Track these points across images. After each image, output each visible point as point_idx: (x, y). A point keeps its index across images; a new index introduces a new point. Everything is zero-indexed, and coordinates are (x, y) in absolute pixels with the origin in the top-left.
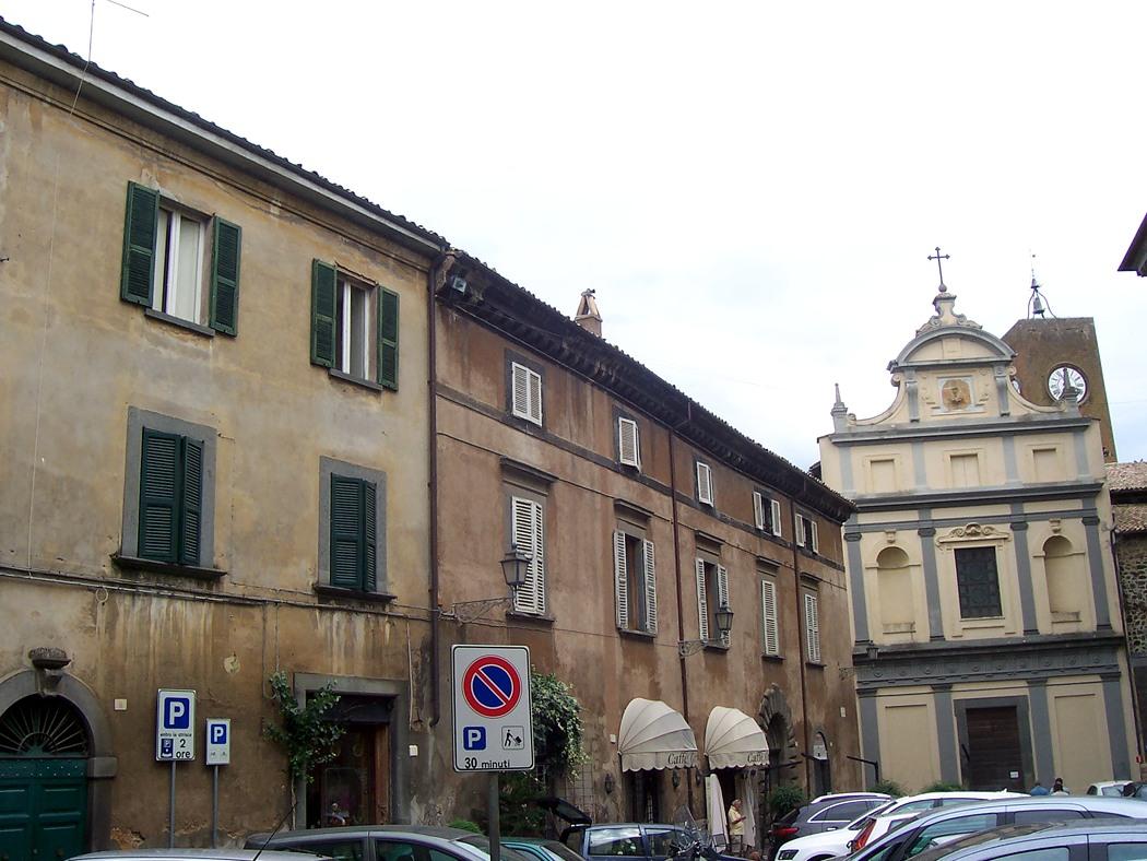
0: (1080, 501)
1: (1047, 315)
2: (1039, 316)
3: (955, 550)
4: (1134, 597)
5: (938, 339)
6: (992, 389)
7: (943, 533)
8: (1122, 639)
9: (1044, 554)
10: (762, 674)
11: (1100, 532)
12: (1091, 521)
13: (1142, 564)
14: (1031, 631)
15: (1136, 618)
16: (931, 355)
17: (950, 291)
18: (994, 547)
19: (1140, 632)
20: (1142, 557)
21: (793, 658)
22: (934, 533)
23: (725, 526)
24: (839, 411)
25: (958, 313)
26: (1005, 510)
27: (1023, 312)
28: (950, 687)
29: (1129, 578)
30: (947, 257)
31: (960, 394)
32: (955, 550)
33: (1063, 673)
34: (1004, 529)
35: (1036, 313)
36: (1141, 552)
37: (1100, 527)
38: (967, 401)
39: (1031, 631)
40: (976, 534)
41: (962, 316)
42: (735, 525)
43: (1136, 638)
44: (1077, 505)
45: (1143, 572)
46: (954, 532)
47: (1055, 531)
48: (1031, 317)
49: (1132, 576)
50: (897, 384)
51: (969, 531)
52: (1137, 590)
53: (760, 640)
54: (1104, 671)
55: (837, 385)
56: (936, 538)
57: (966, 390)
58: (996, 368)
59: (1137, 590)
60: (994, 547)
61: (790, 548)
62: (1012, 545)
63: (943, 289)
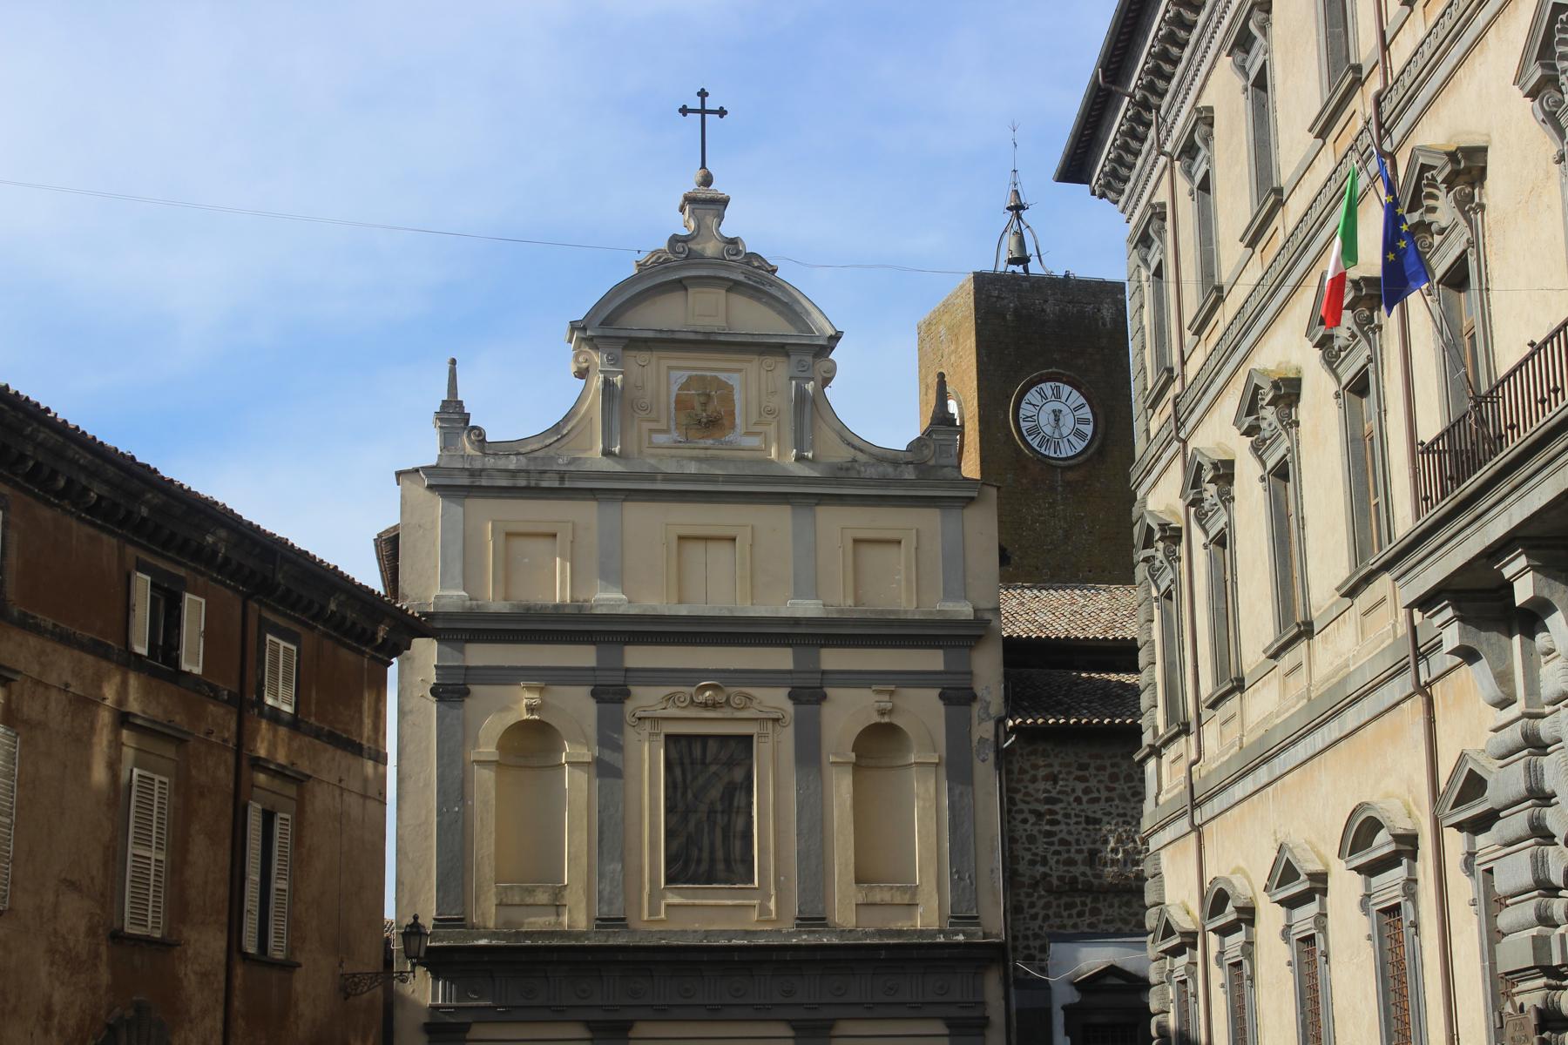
0: (788, 651)
1: (1035, 268)
2: (1019, 269)
3: (668, 737)
4: (1032, 863)
5: (681, 285)
6: (784, 403)
7: (646, 698)
8: (1000, 948)
9: (852, 757)
10: (105, 977)
11: (975, 721)
12: (958, 696)
13: (1054, 794)
14: (812, 920)
15: (1032, 905)
16: (668, 314)
17: (719, 187)
18: (750, 737)
19: (1036, 936)
20: (1055, 781)
21: (208, 944)
22: (627, 694)
23: (33, 641)
24: (453, 416)
25: (730, 235)
26: (781, 659)
27: (992, 258)
28: (830, 1028)
29: (1025, 821)
30: (722, 112)
31: (715, 405)
32: (668, 737)
33: (872, 1011)
34: (776, 699)
35: (1011, 261)
36: (1056, 769)
37: (976, 708)
38: (726, 422)
39: (812, 920)
40: (714, 705)
41: (733, 242)
42: (66, 639)
43: (1027, 947)
44: (932, 660)
45: (1051, 812)
46: (669, 698)
47: (882, 713)
48: (1001, 268)
49: (1032, 819)
50: (582, 374)
51: (701, 699)
52: (1040, 847)
53: (109, 897)
54: (954, 1012)
55: (453, 362)
56: (629, 706)
57: (728, 399)
58: (794, 359)
59: (1040, 847)
60: (750, 737)
61: (228, 702)
62: (787, 735)
63: (707, 180)
